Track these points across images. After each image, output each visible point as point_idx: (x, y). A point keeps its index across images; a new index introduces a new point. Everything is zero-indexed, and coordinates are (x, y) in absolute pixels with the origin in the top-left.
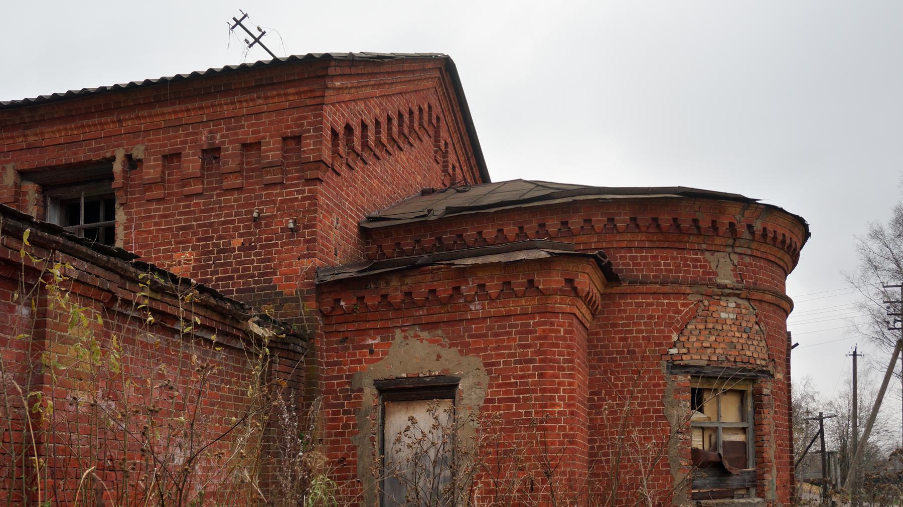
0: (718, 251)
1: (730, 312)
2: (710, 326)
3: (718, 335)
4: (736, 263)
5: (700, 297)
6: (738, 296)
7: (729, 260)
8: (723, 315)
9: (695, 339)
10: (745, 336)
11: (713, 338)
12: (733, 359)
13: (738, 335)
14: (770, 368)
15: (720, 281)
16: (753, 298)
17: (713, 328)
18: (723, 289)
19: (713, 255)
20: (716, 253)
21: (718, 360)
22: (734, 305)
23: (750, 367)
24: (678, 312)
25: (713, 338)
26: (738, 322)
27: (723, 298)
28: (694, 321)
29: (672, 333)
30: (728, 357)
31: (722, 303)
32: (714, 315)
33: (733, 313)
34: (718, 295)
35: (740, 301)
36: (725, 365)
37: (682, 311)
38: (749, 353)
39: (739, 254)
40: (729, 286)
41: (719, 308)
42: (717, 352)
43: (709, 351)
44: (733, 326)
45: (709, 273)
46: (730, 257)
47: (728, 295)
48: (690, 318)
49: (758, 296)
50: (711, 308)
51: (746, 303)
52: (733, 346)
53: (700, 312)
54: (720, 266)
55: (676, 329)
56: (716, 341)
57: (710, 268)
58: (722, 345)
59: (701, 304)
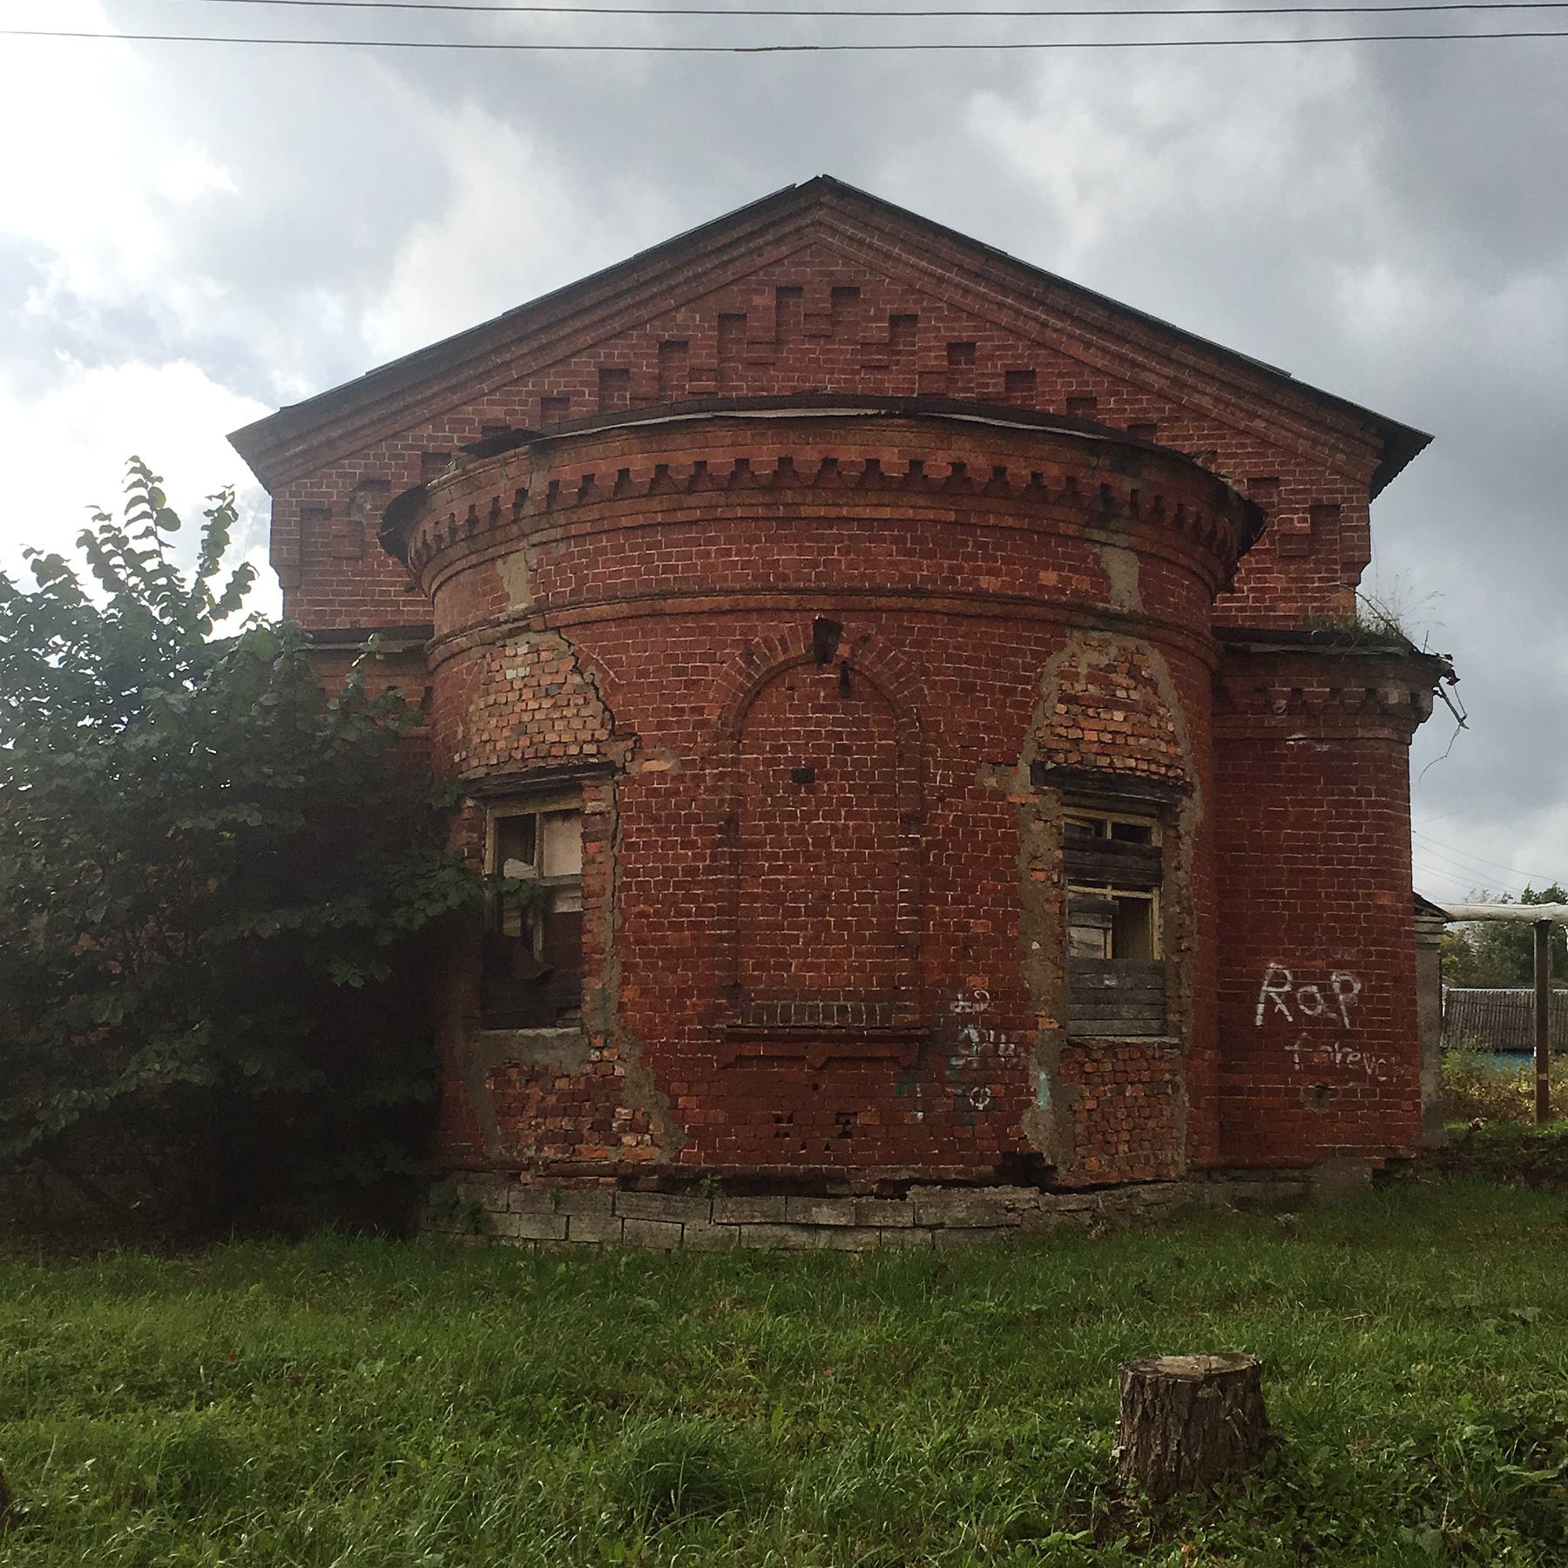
6: (527, 629)
8: (510, 674)
10: (547, 704)
11: (493, 722)
14: (617, 752)
20: (512, 556)
23: (553, 763)
25: (493, 722)
33: (523, 665)
35: (535, 638)
41: (505, 663)
49: (564, 617)
51: (551, 638)
52: (521, 729)
58: (506, 733)
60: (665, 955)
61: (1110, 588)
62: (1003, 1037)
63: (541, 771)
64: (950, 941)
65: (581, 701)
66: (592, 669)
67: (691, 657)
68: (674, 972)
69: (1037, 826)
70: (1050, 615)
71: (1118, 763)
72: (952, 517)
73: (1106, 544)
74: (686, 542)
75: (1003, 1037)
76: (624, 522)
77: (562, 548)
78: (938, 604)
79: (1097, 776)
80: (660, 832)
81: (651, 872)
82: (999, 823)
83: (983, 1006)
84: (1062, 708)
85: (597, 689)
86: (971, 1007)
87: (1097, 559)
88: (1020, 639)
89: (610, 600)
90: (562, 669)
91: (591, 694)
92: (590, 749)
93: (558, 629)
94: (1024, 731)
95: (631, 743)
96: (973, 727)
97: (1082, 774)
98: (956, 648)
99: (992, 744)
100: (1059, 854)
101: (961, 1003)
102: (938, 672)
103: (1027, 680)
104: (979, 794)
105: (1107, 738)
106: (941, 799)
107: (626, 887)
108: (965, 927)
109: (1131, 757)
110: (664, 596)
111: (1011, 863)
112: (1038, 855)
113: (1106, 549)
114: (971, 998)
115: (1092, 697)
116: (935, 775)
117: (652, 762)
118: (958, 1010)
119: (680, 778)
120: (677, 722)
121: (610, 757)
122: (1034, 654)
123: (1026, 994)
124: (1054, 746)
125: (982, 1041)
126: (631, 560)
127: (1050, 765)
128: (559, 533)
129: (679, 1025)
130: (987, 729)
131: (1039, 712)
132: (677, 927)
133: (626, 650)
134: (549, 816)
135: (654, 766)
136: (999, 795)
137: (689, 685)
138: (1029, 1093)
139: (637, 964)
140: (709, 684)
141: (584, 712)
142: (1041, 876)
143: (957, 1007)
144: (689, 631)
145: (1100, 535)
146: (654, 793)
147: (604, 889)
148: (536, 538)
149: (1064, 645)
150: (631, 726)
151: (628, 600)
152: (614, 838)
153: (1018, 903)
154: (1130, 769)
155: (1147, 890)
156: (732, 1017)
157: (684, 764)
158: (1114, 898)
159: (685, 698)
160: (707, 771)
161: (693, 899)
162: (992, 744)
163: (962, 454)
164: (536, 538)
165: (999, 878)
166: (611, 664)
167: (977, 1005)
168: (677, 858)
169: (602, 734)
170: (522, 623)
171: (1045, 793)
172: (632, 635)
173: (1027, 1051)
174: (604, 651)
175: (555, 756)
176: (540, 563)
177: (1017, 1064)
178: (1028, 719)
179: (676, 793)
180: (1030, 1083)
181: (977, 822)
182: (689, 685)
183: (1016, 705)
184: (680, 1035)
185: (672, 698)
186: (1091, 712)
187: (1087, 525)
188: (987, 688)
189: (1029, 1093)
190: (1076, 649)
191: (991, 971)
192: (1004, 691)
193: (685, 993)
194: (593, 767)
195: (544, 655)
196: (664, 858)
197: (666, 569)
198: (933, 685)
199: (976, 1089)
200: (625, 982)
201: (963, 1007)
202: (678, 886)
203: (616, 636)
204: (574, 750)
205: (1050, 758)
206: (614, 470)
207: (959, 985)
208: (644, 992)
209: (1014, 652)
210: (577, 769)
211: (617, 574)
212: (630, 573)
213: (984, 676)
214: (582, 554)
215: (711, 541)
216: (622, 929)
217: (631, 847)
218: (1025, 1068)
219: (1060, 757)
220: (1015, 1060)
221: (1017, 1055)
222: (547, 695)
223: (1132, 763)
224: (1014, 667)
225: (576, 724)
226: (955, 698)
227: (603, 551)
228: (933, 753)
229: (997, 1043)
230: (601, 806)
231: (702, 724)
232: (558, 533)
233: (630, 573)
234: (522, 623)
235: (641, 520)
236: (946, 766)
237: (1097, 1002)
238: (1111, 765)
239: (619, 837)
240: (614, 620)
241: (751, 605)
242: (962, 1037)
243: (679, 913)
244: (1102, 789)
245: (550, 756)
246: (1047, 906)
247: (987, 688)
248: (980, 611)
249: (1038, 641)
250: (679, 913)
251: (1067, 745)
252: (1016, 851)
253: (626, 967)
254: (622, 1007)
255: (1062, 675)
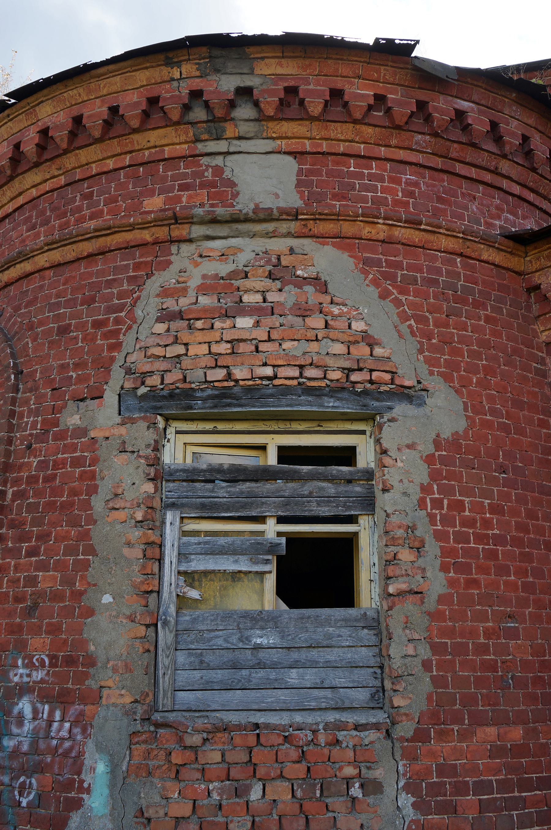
61: (236, 195)
62: (58, 715)
64: (18, 599)
69: (119, 460)
70: (147, 236)
71: (239, 373)
72: (62, 180)
73: (229, 153)
75: (58, 715)
78: (42, 260)
79: (209, 392)
82: (77, 462)
83: (38, 675)
84: (160, 328)
86: (29, 675)
87: (218, 171)
88: (117, 270)
94: (113, 359)
96: (63, 368)
97: (189, 394)
98: (58, 296)
99: (80, 380)
100: (149, 487)
101: (21, 671)
102: (41, 323)
103: (120, 308)
104: (61, 436)
105: (224, 348)
106: (29, 447)
108: (32, 581)
109: (265, 364)
111: (87, 505)
112: (120, 491)
113: (230, 158)
114: (30, 665)
115: (205, 310)
116: (27, 423)
118: (16, 679)
122: (132, 280)
123: (91, 661)
124: (147, 368)
125: (34, 718)
127: (142, 390)
130: (77, 366)
131: (132, 335)
136: (81, 432)
138: (81, 789)
142: (121, 515)
143: (16, 675)
145: (222, 146)
149: (169, 263)
153: (91, 550)
154: (269, 378)
155: (351, 520)
158: (279, 534)
162: (80, 380)
163: (46, 120)
165: (74, 522)
167: (34, 674)
171: (133, 421)
173: (84, 731)
177: (71, 749)
178: (117, 346)
180: (83, 776)
181: (57, 465)
183: (105, 336)
186: (199, 324)
187: (197, 140)
188: (82, 326)
189: (81, 789)
190: (186, 264)
191: (54, 630)
192: (98, 324)
198: (34, 340)
199: (22, 779)
201: (21, 676)
205: (143, 383)
207: (21, 646)
209: (110, 284)
213: (78, 316)
218: (81, 754)
219: (155, 380)
220: (67, 744)
221: (71, 736)
223: (268, 371)
224: (108, 298)
226: (52, 343)
228: (26, 402)
229: (50, 722)
236: (37, 412)
237: (235, 666)
238: (229, 376)
242: (16, 711)
244: (215, 406)
246: (126, 551)
247: (82, 326)
248: (74, 254)
249: (137, 267)
251: (163, 365)
252: (93, 490)
255: (165, 293)
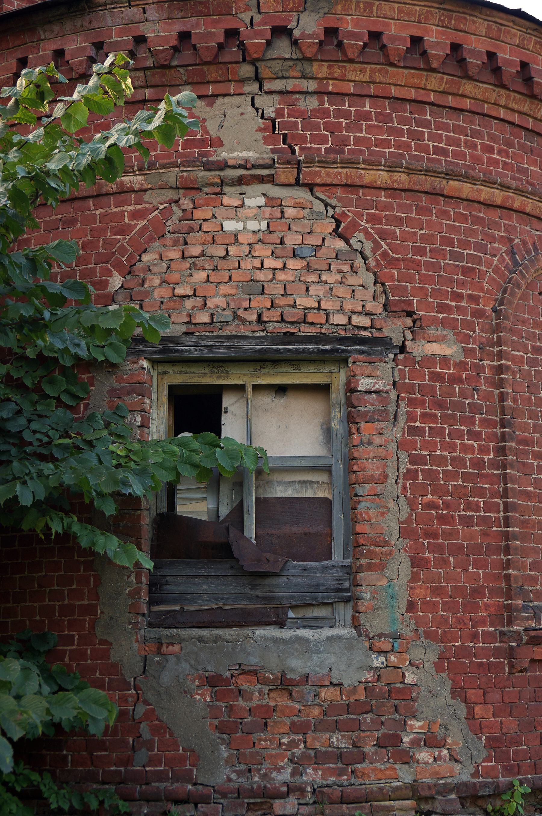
0: (224, 95)
1: (247, 218)
2: (195, 250)
3: (215, 269)
4: (270, 112)
5: (171, 195)
6: (270, 179)
7: (250, 109)
8: (230, 226)
9: (157, 282)
10: (294, 264)
11: (201, 276)
12: (254, 317)
13: (269, 263)
15: (223, 155)
16: (318, 181)
17: (202, 255)
18: (222, 169)
19: (211, 105)
20: (220, 100)
21: (212, 322)
22: (261, 201)
23: (308, 331)
24: (123, 230)
25: (201, 276)
26: (275, 238)
27: (227, 189)
28: (157, 244)
29: (110, 273)
30: (241, 313)
31: (226, 200)
32: (205, 227)
33: (256, 217)
34: (213, 185)
35: (275, 192)
36: (231, 330)
37: (130, 228)
38: (303, 301)
39: (280, 93)
40: (230, 163)
41: (219, 212)
42: (210, 304)
43: (189, 304)
44: (258, 246)
45: (203, 143)
46: (253, 104)
47: (240, 181)
48: (151, 239)
50: (199, 214)
51: (303, 195)
53: (172, 223)
54: (226, 124)
55: (118, 266)
56: (208, 280)
57: (206, 131)
58: (224, 289)
59: (175, 208)
60: (457, 550)
63: (289, 337)
65: (347, 268)
66: (361, 236)
67: (464, 244)
68: (466, 570)
74: (457, 129)
76: (394, 91)
77: (312, 103)
80: (446, 419)
81: (440, 461)
85: (365, 259)
89: (391, 168)
90: (317, 229)
91: (359, 262)
92: (358, 320)
93: (311, 187)
95: (409, 322)
107: (411, 475)
110: (450, 175)
117: (434, 344)
119: (462, 365)
120: (457, 307)
121: (386, 333)
126: (399, 133)
128: (312, 86)
129: (473, 627)
132: (467, 521)
133: (399, 221)
134: (256, 388)
135: (435, 349)
137: (466, 271)
139: (427, 561)
140: (482, 275)
141: (352, 280)
144: (464, 218)
146: (436, 377)
147: (386, 476)
148: (278, 85)
150: (410, 303)
151: (410, 171)
152: (395, 418)
156: (527, 619)
157: (467, 352)
159: (462, 284)
160: (486, 363)
161: (481, 493)
164: (278, 85)
166: (383, 235)
168: (465, 449)
169: (377, 308)
170: (266, 172)
172: (402, 207)
174: (373, 219)
175: (312, 324)
176: (279, 113)
179: (459, 380)
182: (466, 271)
184: (474, 637)
185: (450, 281)
193: (477, 592)
194: (363, 341)
195: (290, 212)
196: (452, 447)
197: (438, 151)
200: (414, 578)
202: (467, 477)
203: (387, 207)
204: (340, 319)
206: (406, 34)
208: (437, 591)
210: (342, 340)
211: (386, 144)
212: (398, 146)
214: (346, 115)
215: (476, 134)
216: (408, 521)
217: (414, 431)
222: (295, 255)
225: (342, 291)
227: (366, 116)
230: (380, 385)
231: (478, 314)
232: (312, 86)
233: (398, 146)
234: (266, 172)
235: (413, 94)
239: (402, 420)
240: (385, 189)
241: (516, 205)
243: (469, 506)
245: (305, 322)
250: (469, 506)
253: (416, 562)
254: (411, 606)
